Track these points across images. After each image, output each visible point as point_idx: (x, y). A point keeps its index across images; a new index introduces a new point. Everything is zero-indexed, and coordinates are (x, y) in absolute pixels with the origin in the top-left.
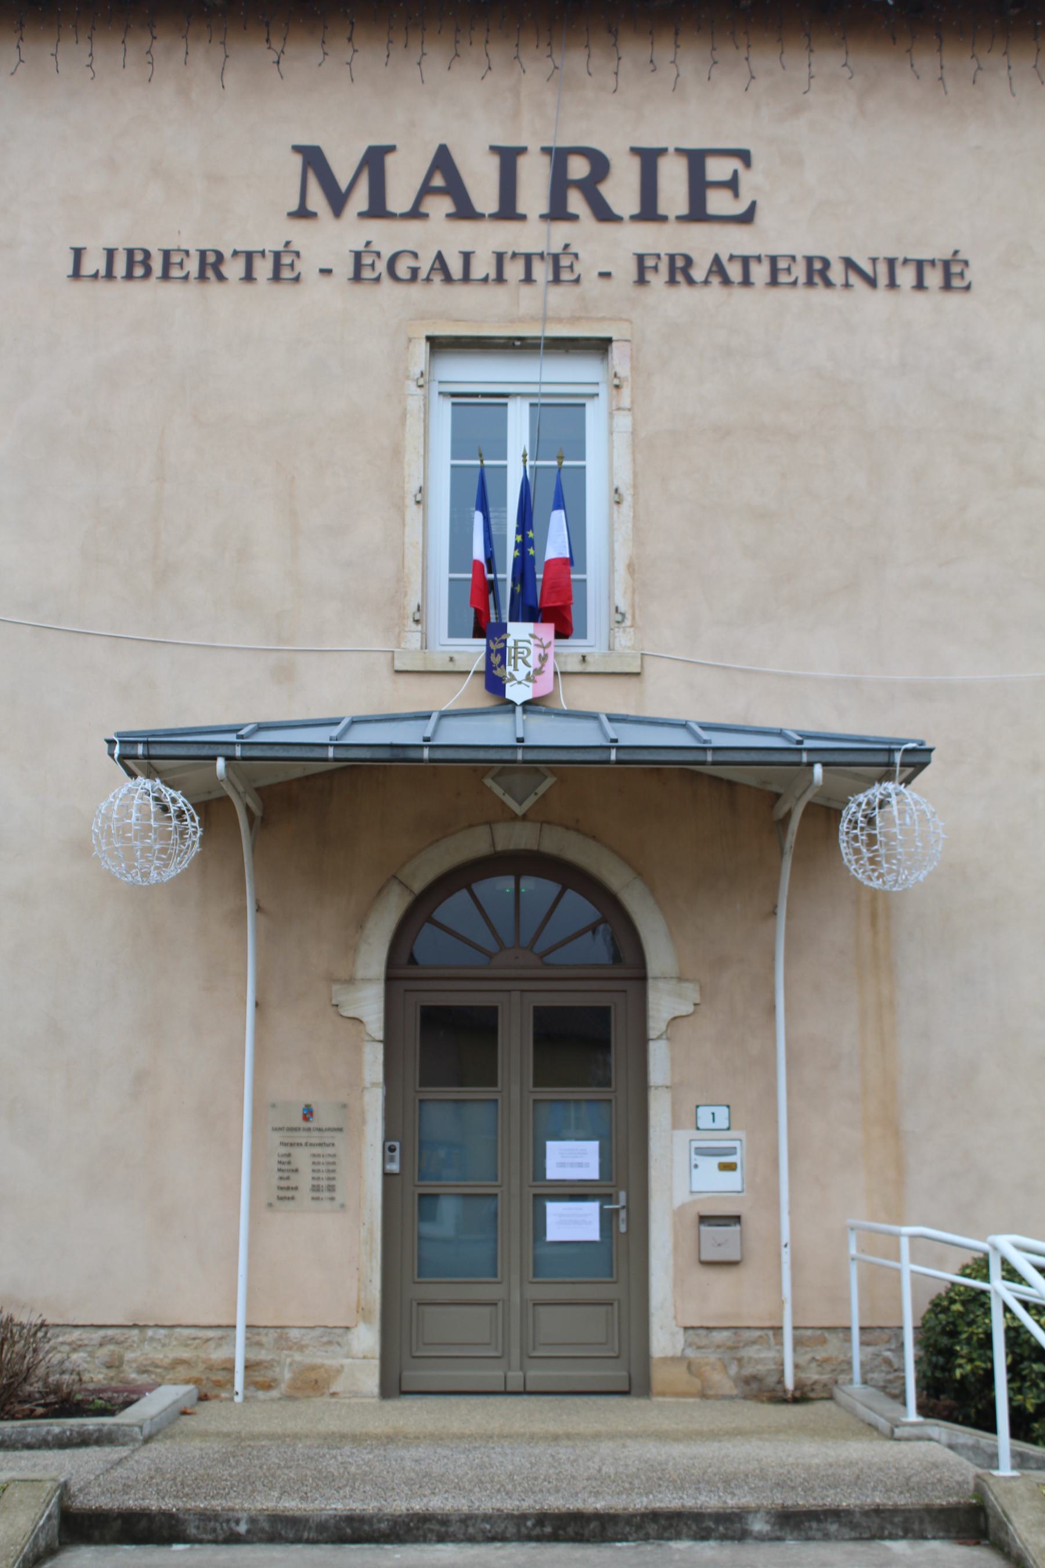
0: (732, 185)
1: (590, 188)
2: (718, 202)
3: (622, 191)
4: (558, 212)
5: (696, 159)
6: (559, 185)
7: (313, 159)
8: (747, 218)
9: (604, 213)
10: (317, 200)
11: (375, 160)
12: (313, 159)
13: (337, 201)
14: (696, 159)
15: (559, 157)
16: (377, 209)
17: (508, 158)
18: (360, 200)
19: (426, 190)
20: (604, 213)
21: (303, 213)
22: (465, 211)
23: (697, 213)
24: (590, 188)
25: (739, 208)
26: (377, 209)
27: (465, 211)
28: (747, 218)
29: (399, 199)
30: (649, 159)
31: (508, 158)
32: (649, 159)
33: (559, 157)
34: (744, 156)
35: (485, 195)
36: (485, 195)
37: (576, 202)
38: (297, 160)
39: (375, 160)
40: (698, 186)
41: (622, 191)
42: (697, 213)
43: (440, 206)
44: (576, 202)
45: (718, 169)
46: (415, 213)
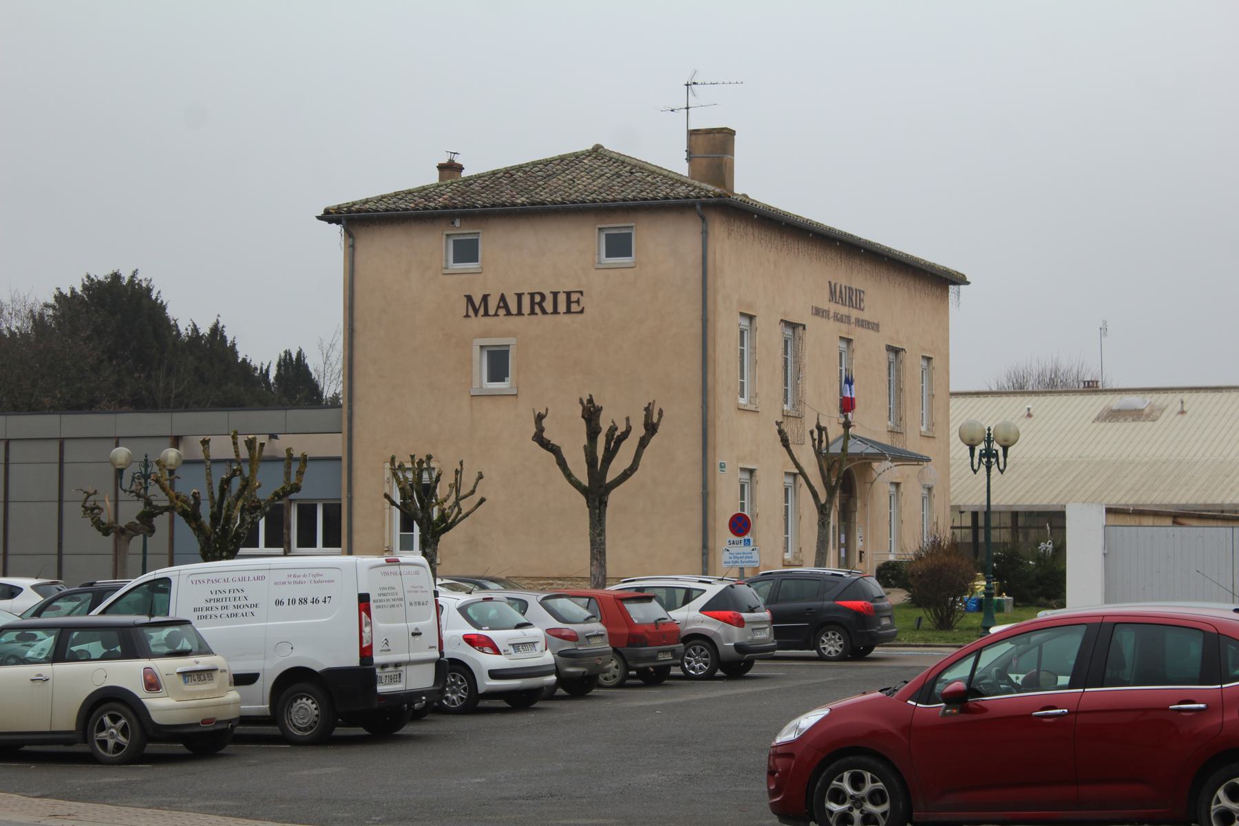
0: (578, 302)
1: (540, 304)
2: (574, 307)
3: (548, 305)
4: (532, 312)
5: (568, 294)
6: (533, 303)
7: (469, 299)
8: (582, 312)
9: (544, 312)
10: (471, 312)
11: (485, 298)
12: (469, 299)
13: (476, 312)
14: (568, 294)
15: (532, 295)
16: (486, 314)
17: (520, 296)
18: (482, 311)
19: (499, 307)
20: (544, 312)
21: (467, 316)
22: (509, 313)
23: (569, 311)
24: (540, 304)
25: (579, 309)
26: (486, 314)
27: (509, 313)
28: (582, 312)
29: (491, 312)
30: (555, 294)
31: (520, 296)
32: (555, 294)
33: (532, 295)
34: (581, 293)
35: (514, 310)
36: (514, 310)
37: (537, 309)
38: (465, 300)
39: (485, 298)
40: (569, 302)
41: (548, 305)
42: (569, 311)
43: (502, 312)
44: (537, 309)
45: (574, 297)
46: (496, 315)
